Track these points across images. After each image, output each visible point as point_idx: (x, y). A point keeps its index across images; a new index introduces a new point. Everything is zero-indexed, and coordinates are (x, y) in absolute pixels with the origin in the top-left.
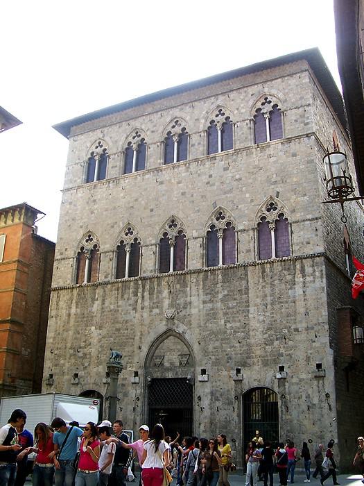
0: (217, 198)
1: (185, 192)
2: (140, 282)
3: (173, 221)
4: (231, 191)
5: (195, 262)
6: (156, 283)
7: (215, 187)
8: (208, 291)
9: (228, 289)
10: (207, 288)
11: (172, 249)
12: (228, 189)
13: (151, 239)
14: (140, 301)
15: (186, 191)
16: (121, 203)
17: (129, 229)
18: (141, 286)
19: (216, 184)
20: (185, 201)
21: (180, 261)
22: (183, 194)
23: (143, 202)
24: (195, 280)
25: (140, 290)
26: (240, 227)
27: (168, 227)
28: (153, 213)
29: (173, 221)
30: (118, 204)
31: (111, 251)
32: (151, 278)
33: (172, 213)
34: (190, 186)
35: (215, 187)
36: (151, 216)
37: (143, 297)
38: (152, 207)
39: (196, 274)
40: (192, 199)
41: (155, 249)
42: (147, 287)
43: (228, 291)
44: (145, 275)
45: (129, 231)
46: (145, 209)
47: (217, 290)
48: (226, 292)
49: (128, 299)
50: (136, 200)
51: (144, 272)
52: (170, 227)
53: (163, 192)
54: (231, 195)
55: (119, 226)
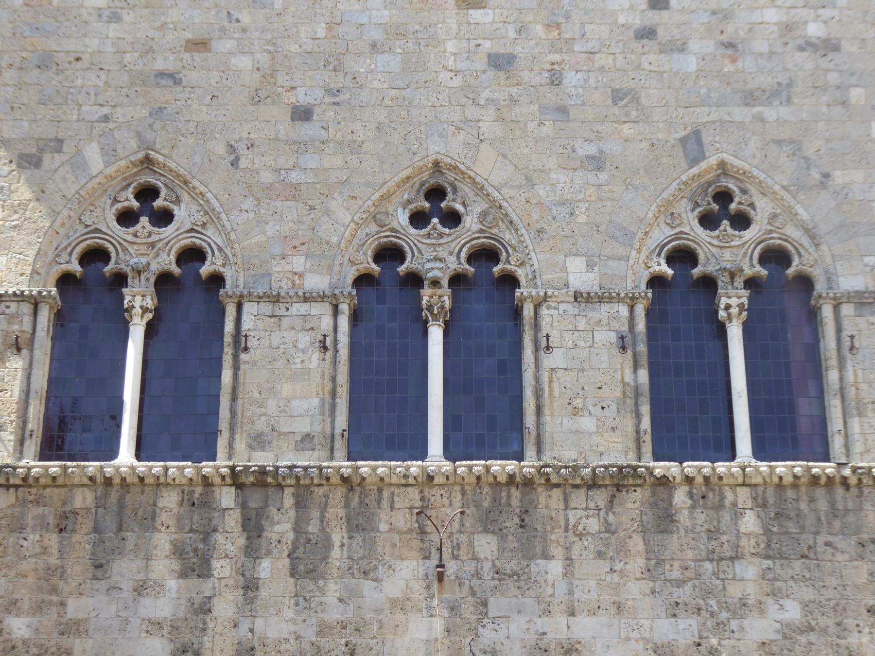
0: (702, 115)
1: (511, 59)
2: (227, 497)
3: (436, 193)
4: (781, 93)
5: (587, 423)
6: (336, 511)
7: (691, 64)
8: (685, 593)
9: (808, 594)
10: (676, 574)
11: (436, 335)
12: (765, 81)
13: (298, 263)
14: (225, 608)
15: (518, 50)
16: (94, 43)
17: (147, 194)
18: (233, 521)
19: (695, 46)
20: (513, 101)
21: (491, 415)
22: (500, 62)
23: (243, 63)
24: (593, 525)
25: (230, 540)
26: (850, 281)
27: (403, 218)
28: (306, 130)
29: (436, 193)
30: (72, 45)
31: (19, 297)
32: (304, 487)
33: (436, 149)
34: (539, 30)
35: (691, 64)
36: (301, 146)
37: (250, 586)
38: (301, 97)
39: (600, 498)
40: (551, 97)
41: (326, 323)
42: (281, 527)
43: (805, 605)
44: (263, 459)
45: (147, 204)
46: (256, 99)
47: (735, 591)
48: (793, 612)
49: (140, 589)
50: (200, 45)
51: (258, 442)
52: (419, 219)
53: (377, 35)
54: (784, 112)
55: (78, 164)
